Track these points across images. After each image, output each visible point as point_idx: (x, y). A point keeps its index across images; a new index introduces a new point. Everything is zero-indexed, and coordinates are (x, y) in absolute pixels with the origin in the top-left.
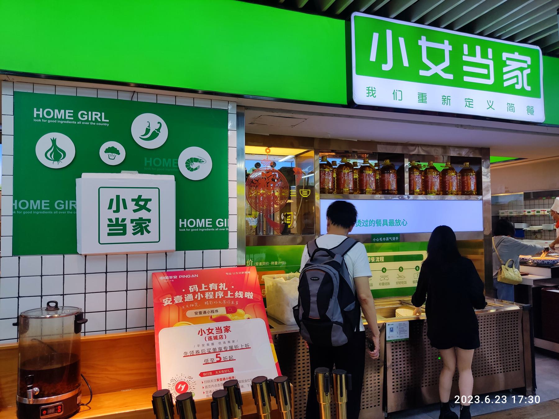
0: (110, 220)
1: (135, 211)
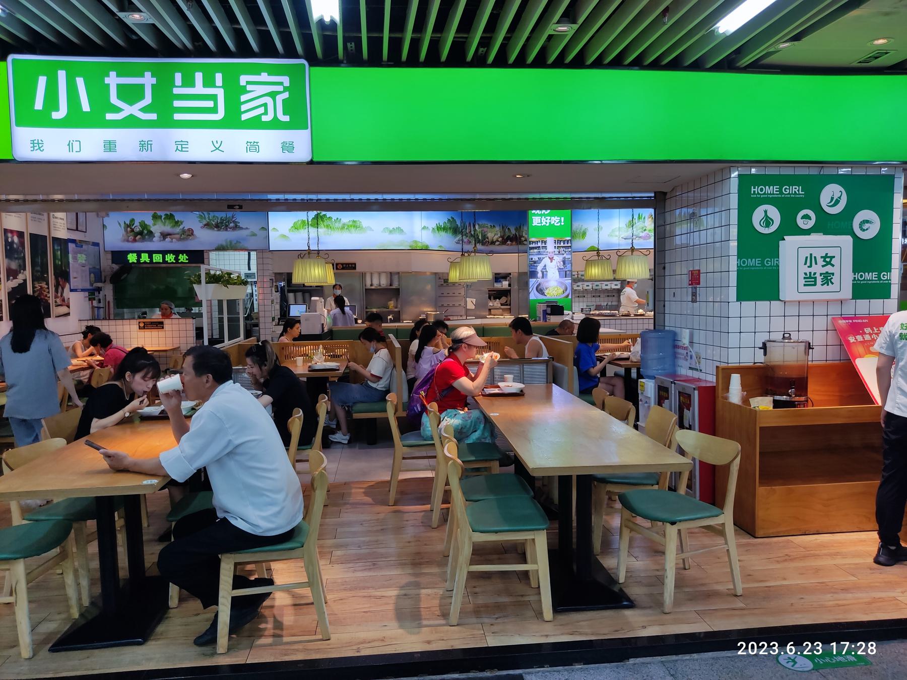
0: (806, 274)
1: (823, 266)
